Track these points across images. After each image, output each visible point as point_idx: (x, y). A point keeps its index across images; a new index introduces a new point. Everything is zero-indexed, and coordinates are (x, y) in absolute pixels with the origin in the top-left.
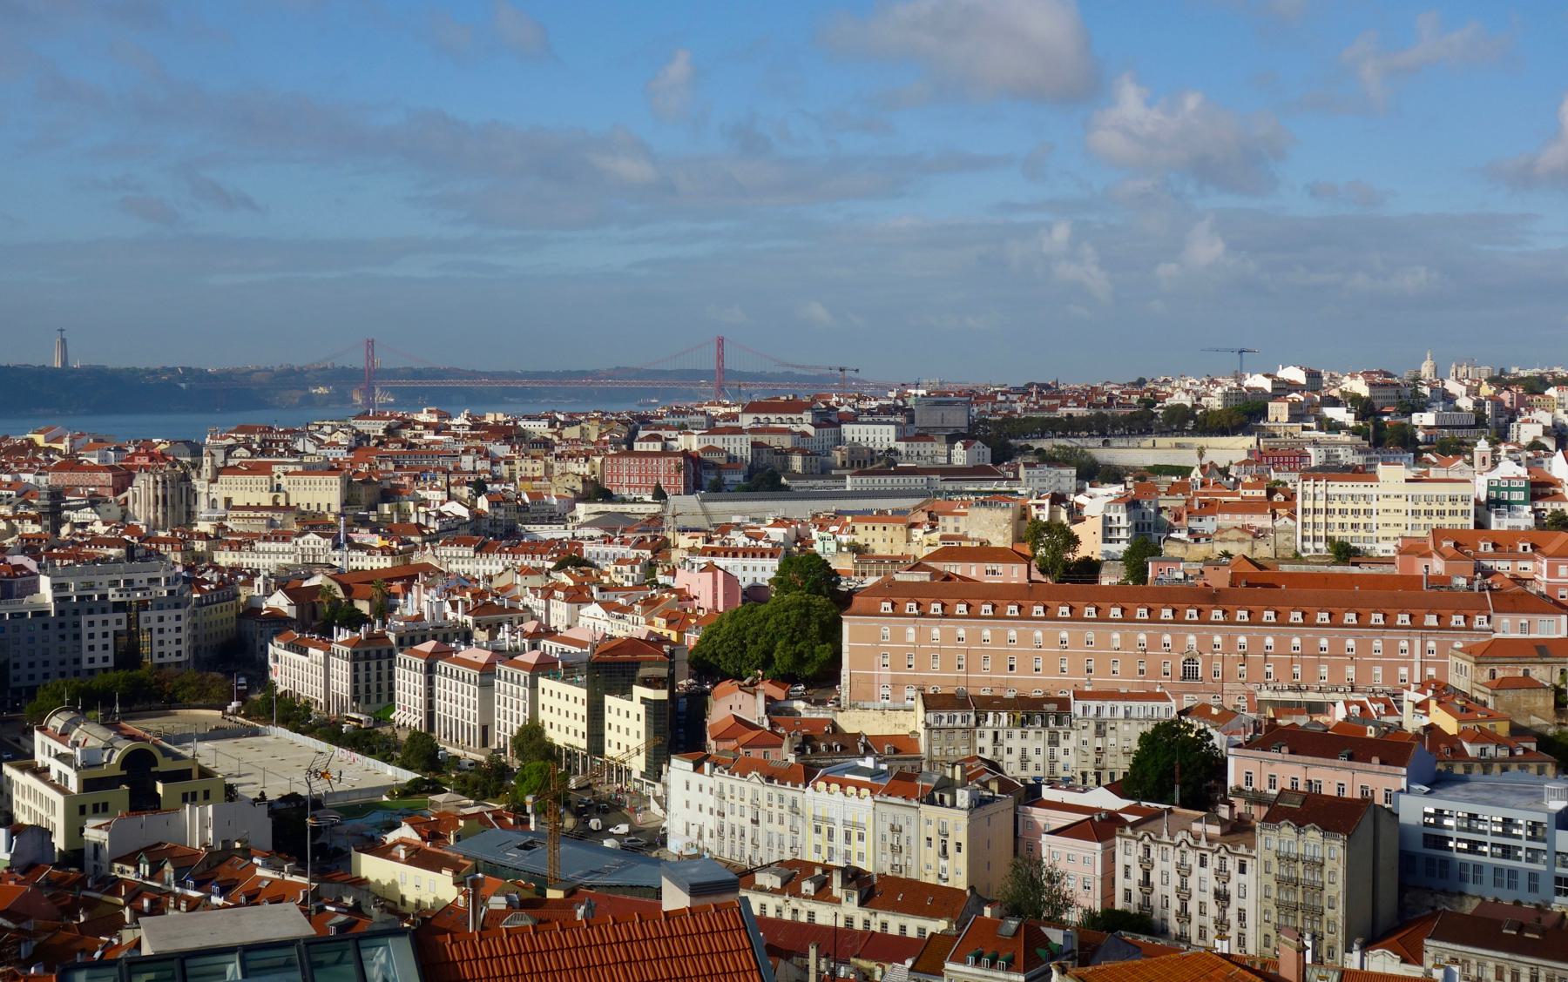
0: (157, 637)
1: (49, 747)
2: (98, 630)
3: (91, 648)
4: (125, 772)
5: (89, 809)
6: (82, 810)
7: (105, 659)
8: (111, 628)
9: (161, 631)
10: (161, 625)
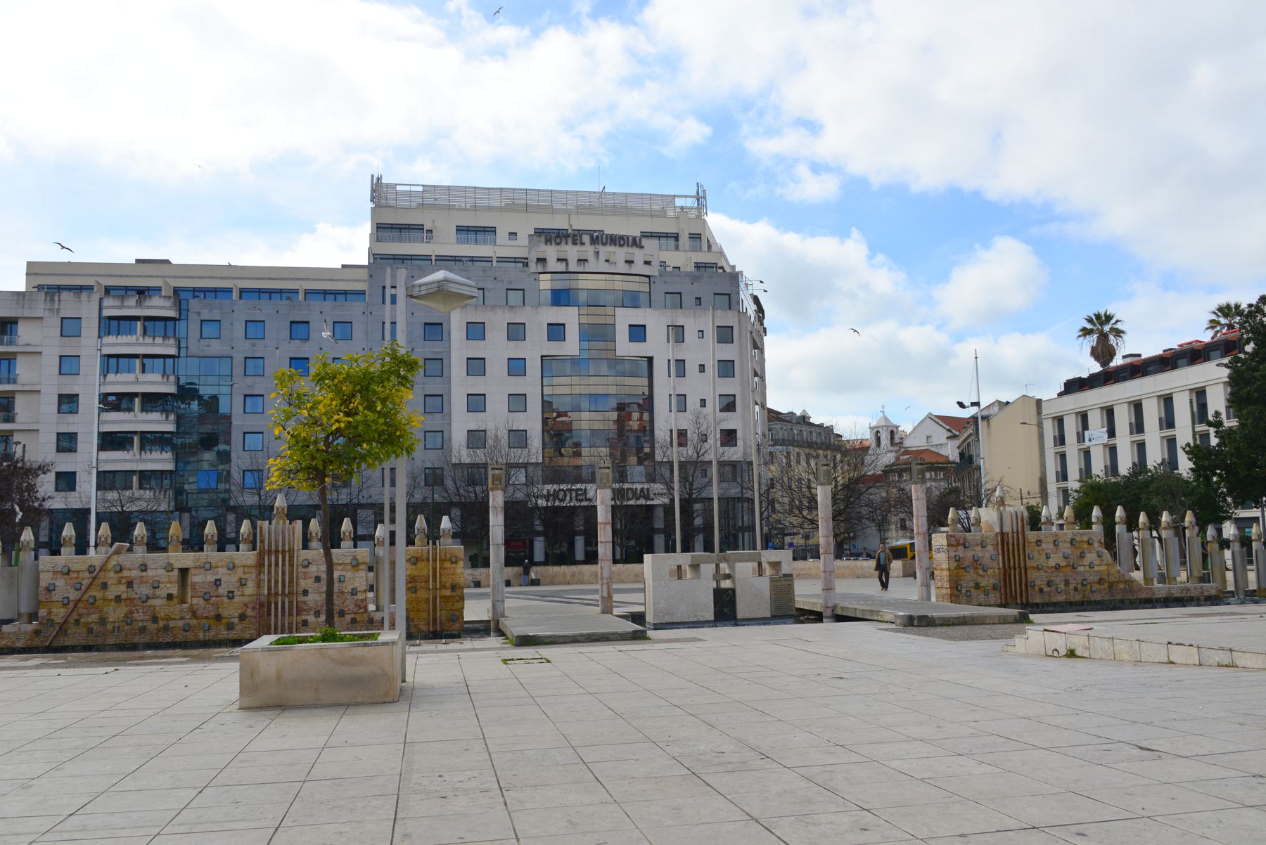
0: (664, 387)
2: (497, 349)
3: (477, 402)
8: (535, 347)
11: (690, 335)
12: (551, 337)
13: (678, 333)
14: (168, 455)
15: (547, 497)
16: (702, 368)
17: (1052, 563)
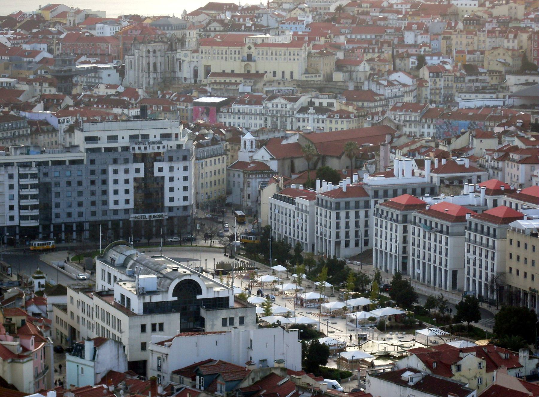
0: (167, 185)
1: (109, 274)
2: (122, 177)
4: (176, 299)
5: (149, 328)
6: (143, 328)
8: (132, 176)
9: (171, 179)
10: (170, 174)
11: (175, 169)
12: (136, 172)
13: (171, 169)
14: (38, 211)
15: (135, 217)
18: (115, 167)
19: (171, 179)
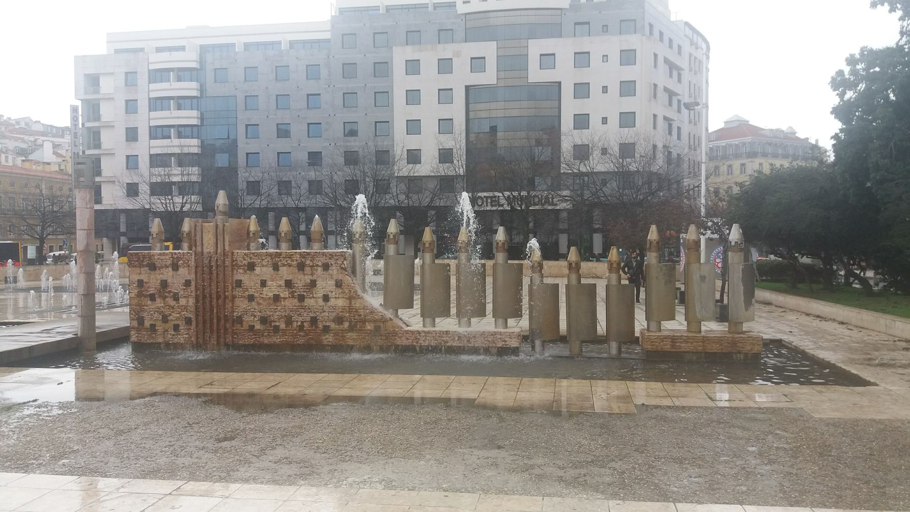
7: (446, 156)
10: (583, 76)
11: (595, 59)
16: (605, 89)
17: (268, 293)
18: (410, 53)
19: (582, 91)
